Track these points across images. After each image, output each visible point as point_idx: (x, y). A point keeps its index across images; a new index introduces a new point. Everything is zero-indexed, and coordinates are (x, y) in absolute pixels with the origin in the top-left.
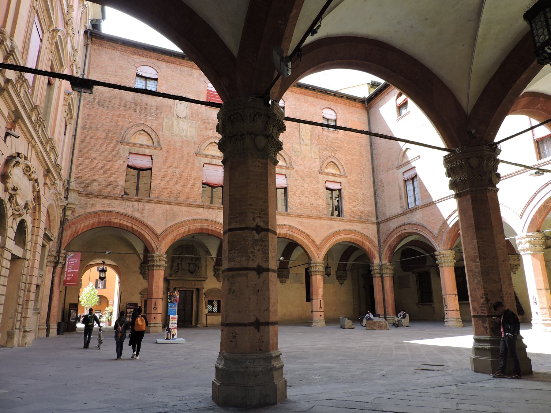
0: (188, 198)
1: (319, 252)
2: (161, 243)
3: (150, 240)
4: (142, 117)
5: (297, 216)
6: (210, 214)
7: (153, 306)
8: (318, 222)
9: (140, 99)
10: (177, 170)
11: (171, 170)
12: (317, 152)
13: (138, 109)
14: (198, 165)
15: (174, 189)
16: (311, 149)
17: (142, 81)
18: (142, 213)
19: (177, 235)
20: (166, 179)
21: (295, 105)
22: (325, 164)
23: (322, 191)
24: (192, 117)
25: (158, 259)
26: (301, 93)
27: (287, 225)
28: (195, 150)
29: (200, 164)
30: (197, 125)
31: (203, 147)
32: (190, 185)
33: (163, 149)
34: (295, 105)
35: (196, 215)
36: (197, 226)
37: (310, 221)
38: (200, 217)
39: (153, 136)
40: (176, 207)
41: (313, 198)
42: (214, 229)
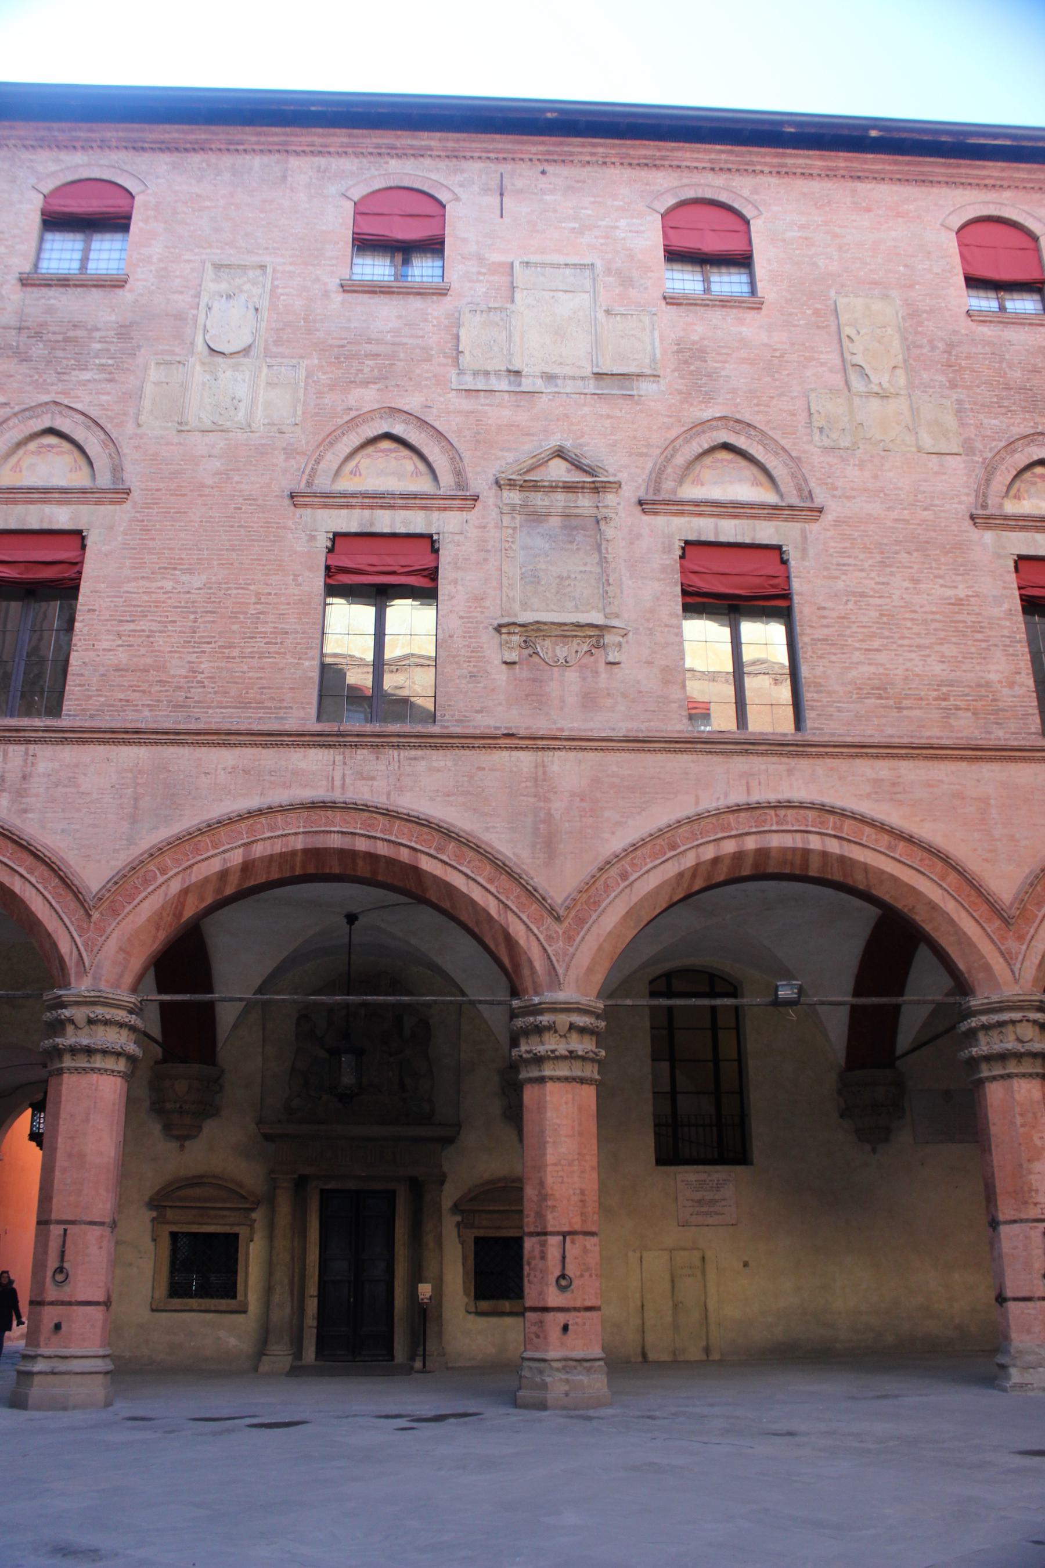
0: (245, 705)
1: (1011, 944)
2: (101, 931)
3: (51, 924)
4: (52, 378)
5: (861, 750)
6: (362, 776)
7: (52, 1264)
8: (991, 772)
9: (50, 310)
10: (198, 581)
11: (168, 585)
12: (950, 420)
13: (38, 350)
14: (301, 546)
15: (177, 668)
16: (914, 411)
17: (69, 245)
18: (20, 793)
19: (185, 892)
20: (144, 625)
21: (802, 227)
22: (1002, 478)
23: (998, 612)
24: (276, 343)
25: (79, 1014)
26: (830, 174)
27: (801, 806)
28: (288, 484)
29: (312, 538)
30: (302, 374)
31: (332, 459)
32: (260, 644)
33: (135, 494)
34: (802, 227)
35: (287, 786)
36: (292, 837)
37: (944, 772)
38: (307, 794)
39: (93, 444)
40: (185, 751)
41: (949, 650)
42: (382, 849)
